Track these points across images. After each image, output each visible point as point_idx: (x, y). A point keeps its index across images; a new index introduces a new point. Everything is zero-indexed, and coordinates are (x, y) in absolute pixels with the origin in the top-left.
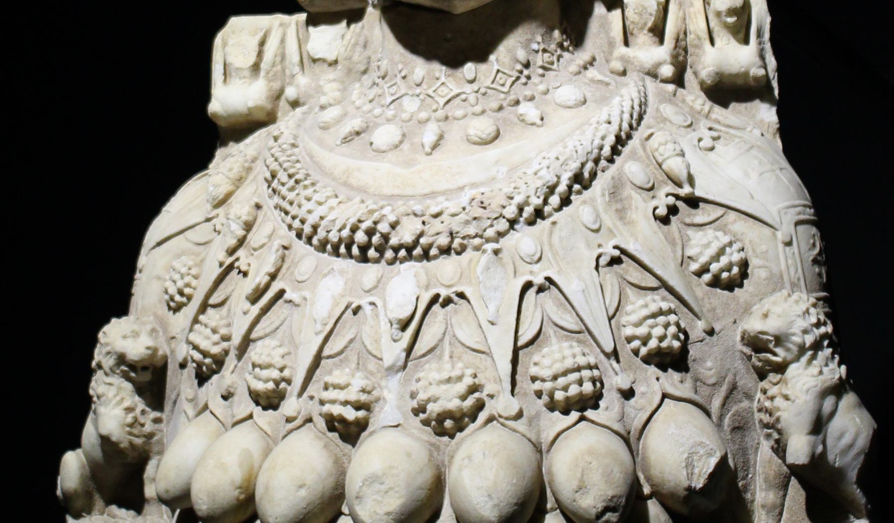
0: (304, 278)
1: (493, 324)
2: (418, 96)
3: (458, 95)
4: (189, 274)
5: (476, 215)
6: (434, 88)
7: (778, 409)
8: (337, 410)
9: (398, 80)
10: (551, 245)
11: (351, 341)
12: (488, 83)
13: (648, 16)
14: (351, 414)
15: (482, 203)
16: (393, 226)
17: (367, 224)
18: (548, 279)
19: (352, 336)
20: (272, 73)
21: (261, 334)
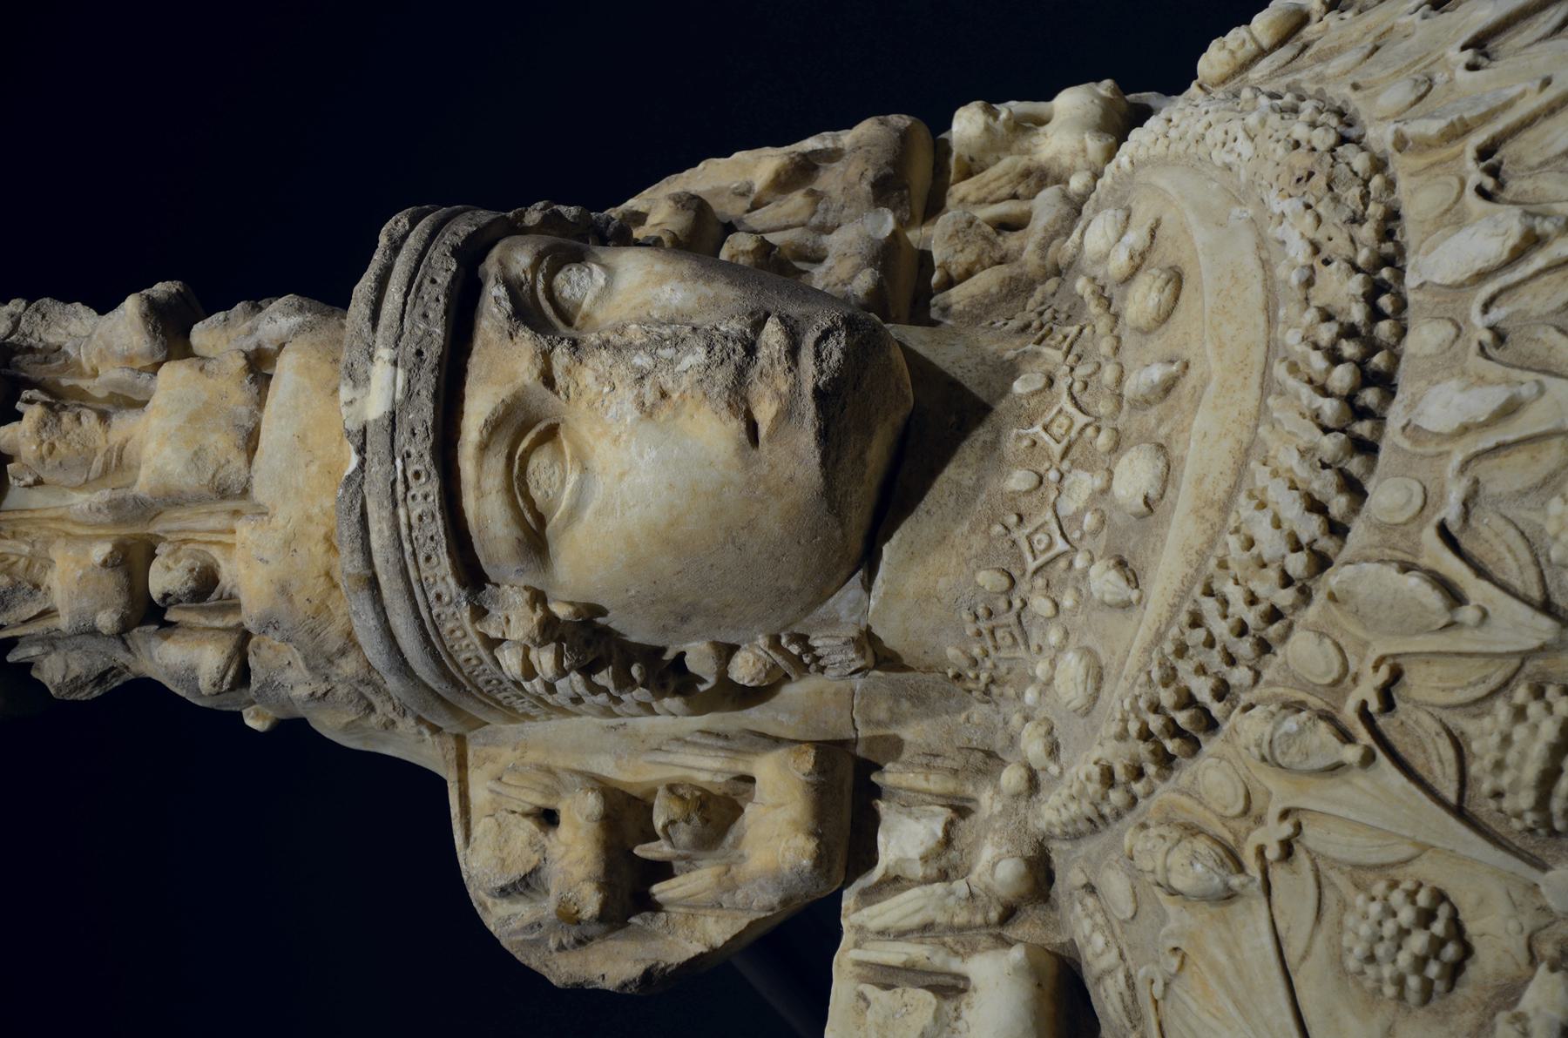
0: (1417, 489)
1: (1547, 82)
2: (1062, 476)
3: (1073, 398)
4: (1386, 899)
5: (1323, 184)
6: (1052, 443)
9: (1020, 535)
12: (1057, 356)
13: (971, 231)
15: (1299, 180)
16: (1327, 316)
17: (1318, 361)
19: (1552, 330)
20: (958, 947)
21: (1531, 574)
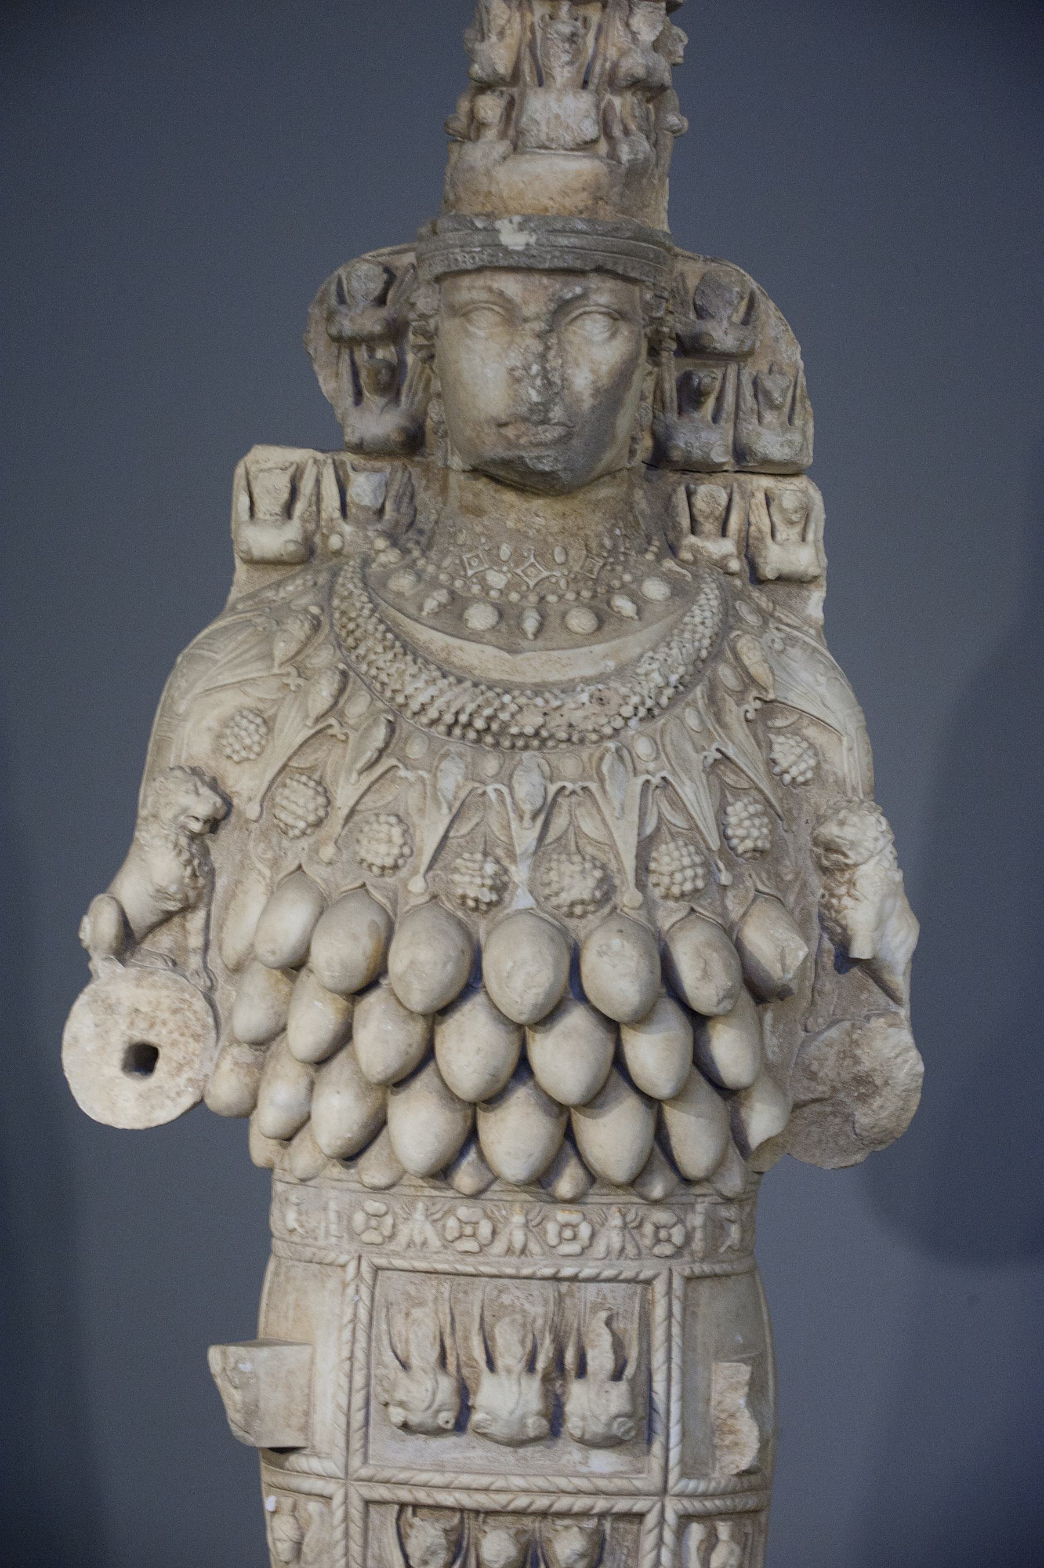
7: (846, 908)
8: (472, 893)
10: (663, 745)
11: (477, 824)
14: (488, 896)
17: (488, 712)
18: (664, 778)
